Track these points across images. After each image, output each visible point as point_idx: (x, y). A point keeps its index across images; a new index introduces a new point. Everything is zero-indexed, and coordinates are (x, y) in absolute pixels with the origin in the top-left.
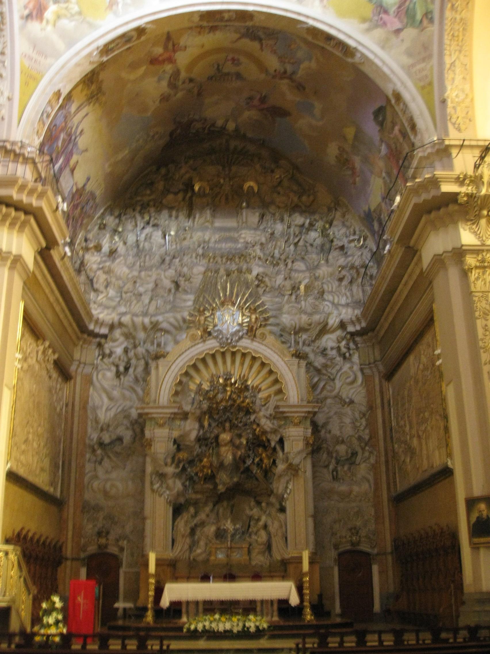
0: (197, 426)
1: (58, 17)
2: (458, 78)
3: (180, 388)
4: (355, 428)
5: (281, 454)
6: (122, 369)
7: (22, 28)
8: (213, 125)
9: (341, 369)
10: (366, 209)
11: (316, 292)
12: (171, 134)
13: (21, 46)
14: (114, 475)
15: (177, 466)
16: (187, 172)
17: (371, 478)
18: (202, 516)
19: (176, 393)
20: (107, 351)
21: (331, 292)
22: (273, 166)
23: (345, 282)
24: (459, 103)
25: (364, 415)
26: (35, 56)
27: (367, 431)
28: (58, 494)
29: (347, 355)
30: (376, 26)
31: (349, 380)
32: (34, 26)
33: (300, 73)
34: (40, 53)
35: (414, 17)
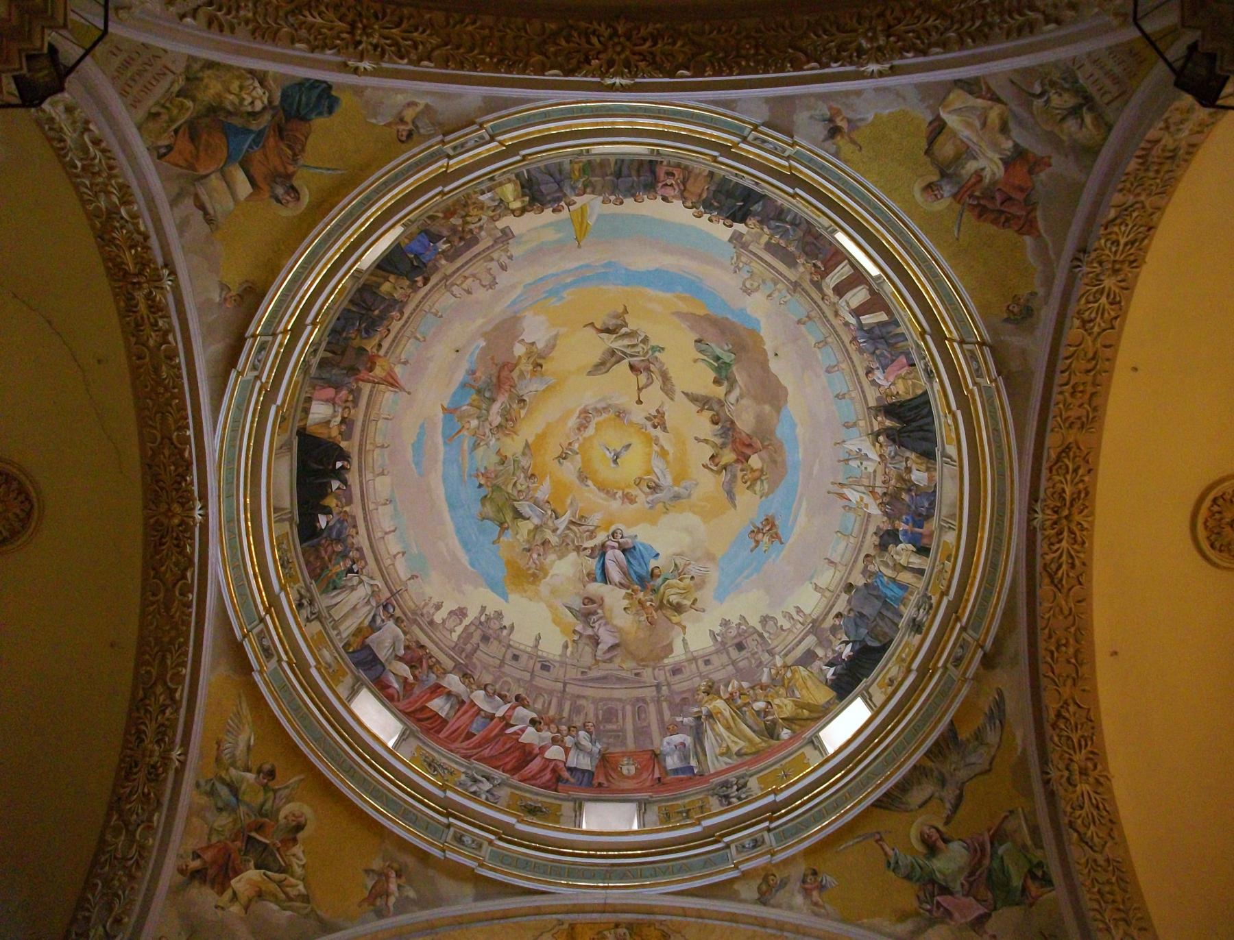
1: (260, 895)
30: (932, 922)
32: (204, 897)
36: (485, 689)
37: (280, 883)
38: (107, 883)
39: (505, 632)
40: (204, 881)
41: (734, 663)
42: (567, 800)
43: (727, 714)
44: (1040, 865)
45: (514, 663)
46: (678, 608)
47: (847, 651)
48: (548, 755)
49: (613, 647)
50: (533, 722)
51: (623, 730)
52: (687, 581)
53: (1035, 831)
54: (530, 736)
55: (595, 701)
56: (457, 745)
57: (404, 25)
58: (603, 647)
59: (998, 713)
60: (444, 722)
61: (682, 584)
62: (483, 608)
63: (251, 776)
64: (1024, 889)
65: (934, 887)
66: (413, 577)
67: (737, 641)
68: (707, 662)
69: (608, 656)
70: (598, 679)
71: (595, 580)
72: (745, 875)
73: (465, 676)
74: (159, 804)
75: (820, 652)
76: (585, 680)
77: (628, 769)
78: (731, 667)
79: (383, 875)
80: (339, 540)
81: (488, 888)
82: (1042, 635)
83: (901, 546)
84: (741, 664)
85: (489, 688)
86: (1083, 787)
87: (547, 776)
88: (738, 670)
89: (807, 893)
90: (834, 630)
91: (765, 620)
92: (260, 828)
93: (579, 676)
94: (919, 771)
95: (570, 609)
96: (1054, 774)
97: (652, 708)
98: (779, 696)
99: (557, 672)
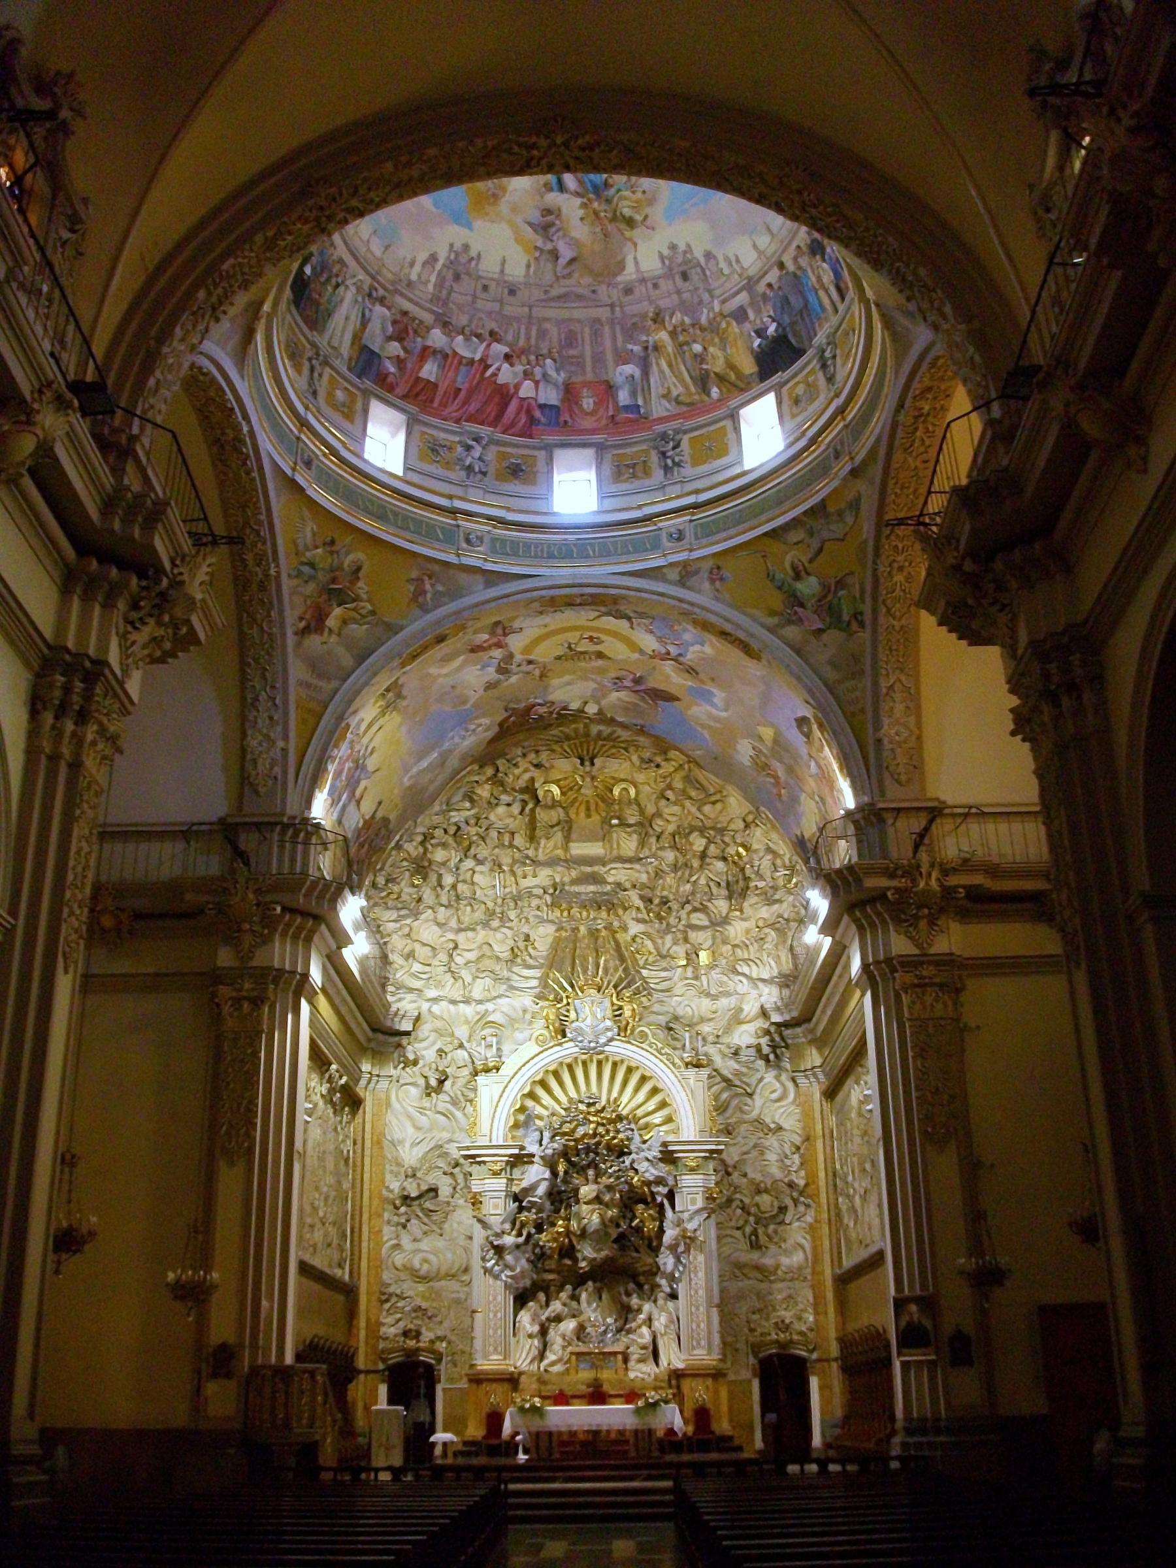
0: (547, 1175)
1: (345, 622)
2: (899, 709)
3: (523, 1119)
4: (785, 1168)
5: (669, 1213)
6: (433, 1083)
7: (298, 645)
9: (761, 1080)
12: (501, 725)
13: (297, 671)
14: (425, 1245)
15: (520, 1235)
16: (526, 771)
17: (807, 1246)
18: (556, 1306)
19: (516, 1126)
20: (411, 1057)
24: (899, 744)
25: (798, 1148)
26: (315, 681)
27: (803, 1173)
28: (347, 1277)
29: (772, 1057)
30: (789, 622)
31: (775, 1096)
32: (314, 642)
33: (689, 656)
34: (320, 676)
35: (840, 616)
36: (463, 333)
37: (354, 609)
38: (256, 660)
39: (473, 263)
40: (310, 632)
41: (679, 292)
42: (540, 448)
43: (670, 349)
44: (861, 614)
45: (484, 295)
46: (630, 223)
47: (772, 329)
48: (523, 393)
49: (573, 260)
50: (507, 357)
51: (582, 356)
52: (639, 195)
53: (862, 591)
54: (506, 374)
55: (559, 322)
56: (450, 409)
57: (361, 192)
58: (562, 261)
59: (855, 505)
60: (435, 386)
61: (634, 197)
62: (452, 245)
63: (319, 551)
64: (849, 624)
65: (796, 601)
66: (387, 247)
67: (682, 268)
68: (655, 286)
69: (567, 271)
70: (559, 297)
71: (551, 190)
72: (671, 565)
73: (445, 324)
74: (271, 603)
75: (751, 315)
76: (548, 300)
77: (588, 403)
78: (675, 297)
79: (419, 580)
80: (322, 271)
81: (492, 578)
82: (891, 483)
83: (825, 265)
84: (686, 296)
85: (467, 331)
86: (899, 578)
87: (523, 419)
88: (682, 302)
89: (712, 581)
90: (765, 297)
91: (708, 255)
92: (334, 580)
93: (543, 297)
94: (795, 523)
95: (530, 224)
96: (881, 568)
97: (607, 329)
98: (714, 345)
99: (523, 295)
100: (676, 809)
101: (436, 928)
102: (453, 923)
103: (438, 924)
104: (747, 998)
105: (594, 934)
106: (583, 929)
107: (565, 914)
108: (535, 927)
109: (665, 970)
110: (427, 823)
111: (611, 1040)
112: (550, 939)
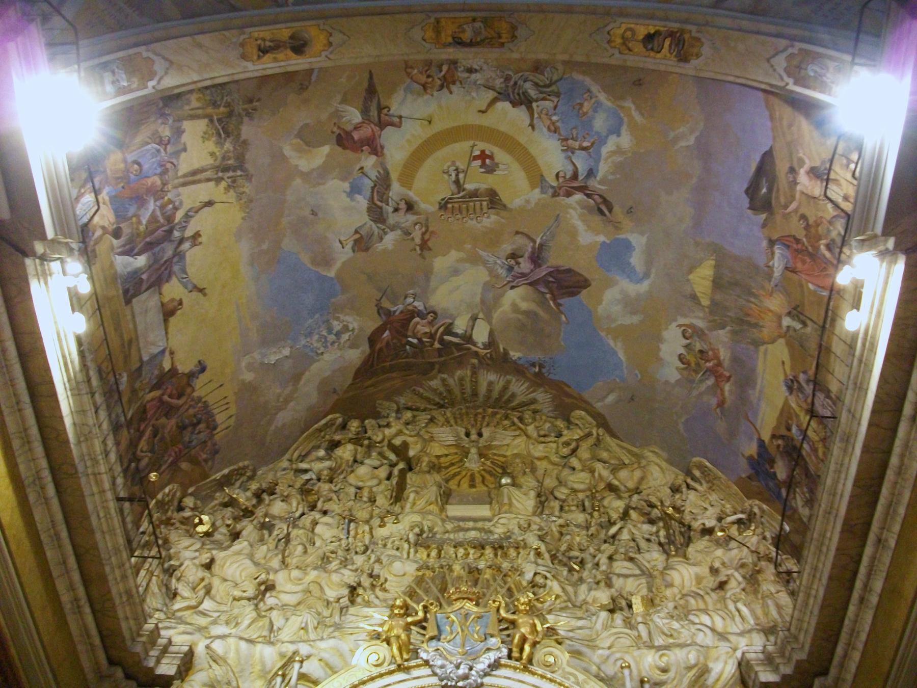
8: (449, 330)
10: (752, 449)
11: (671, 605)
12: (373, 340)
16: (399, 433)
21: (705, 611)
22: (560, 424)
23: (734, 587)
100: (585, 476)
101: (248, 562)
102: (275, 563)
103: (256, 564)
104: (713, 653)
105: (473, 572)
106: (457, 568)
107: (434, 553)
108: (391, 563)
109: (580, 618)
110: (270, 477)
111: (496, 665)
112: (408, 580)
